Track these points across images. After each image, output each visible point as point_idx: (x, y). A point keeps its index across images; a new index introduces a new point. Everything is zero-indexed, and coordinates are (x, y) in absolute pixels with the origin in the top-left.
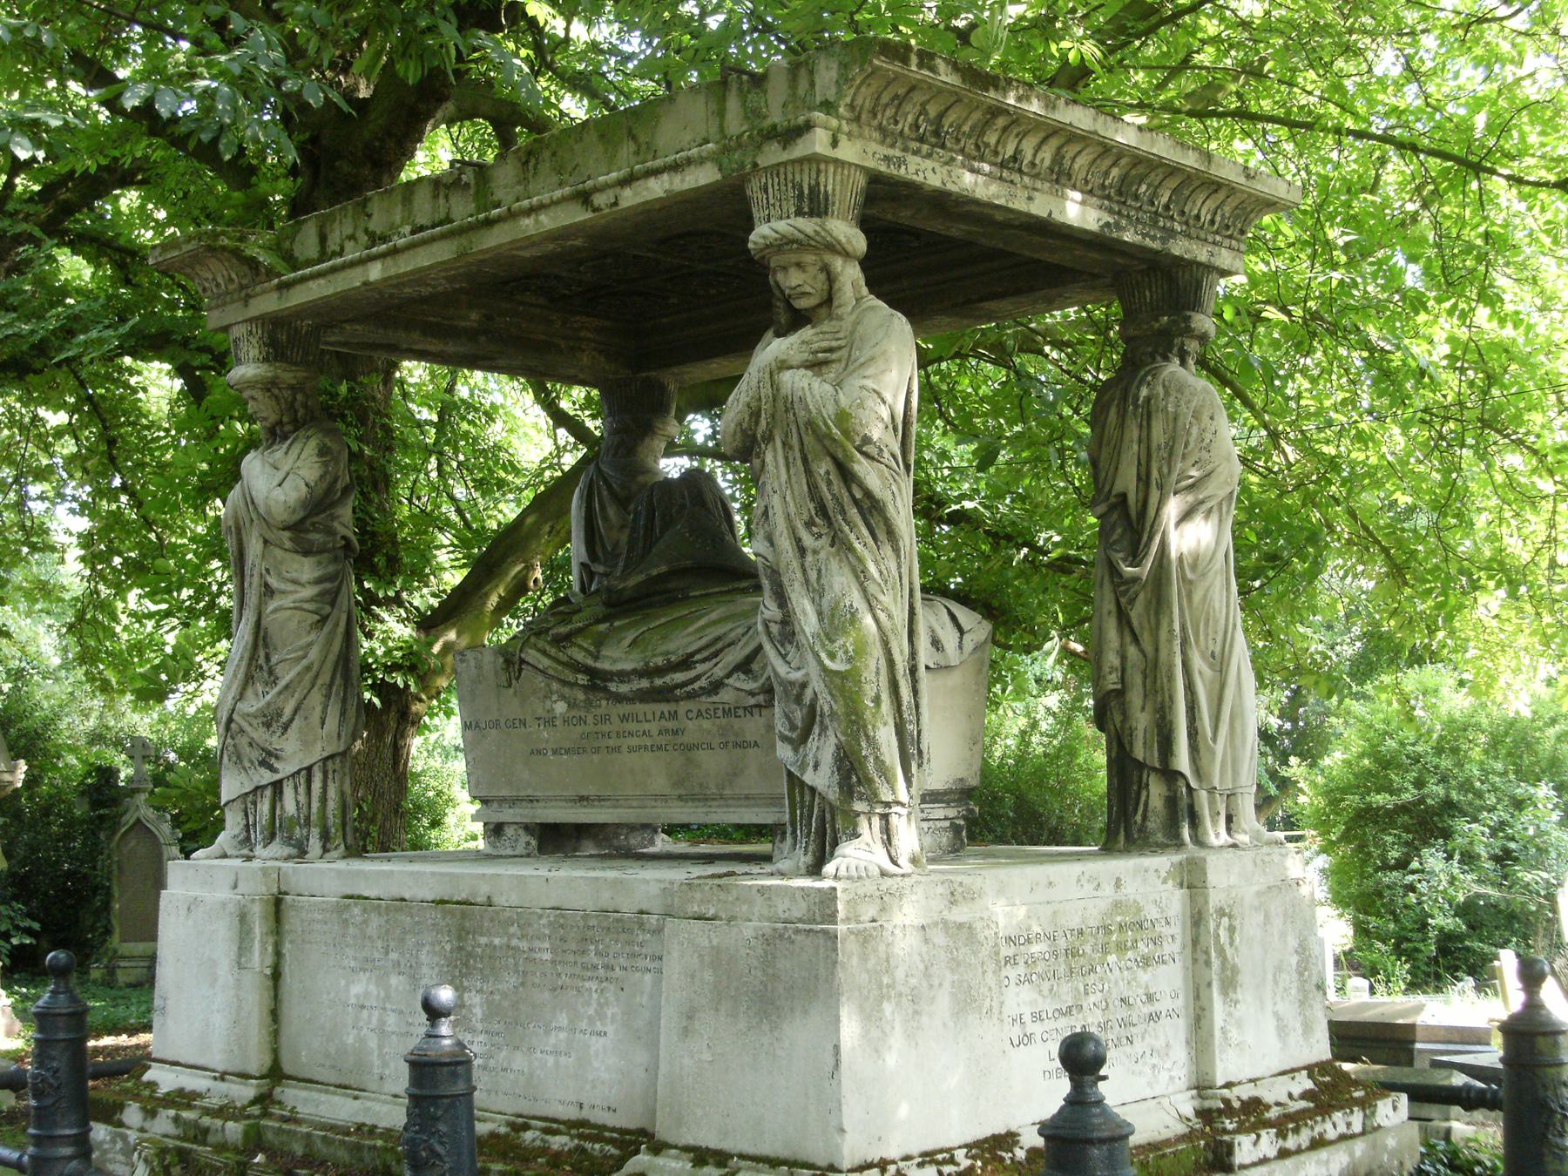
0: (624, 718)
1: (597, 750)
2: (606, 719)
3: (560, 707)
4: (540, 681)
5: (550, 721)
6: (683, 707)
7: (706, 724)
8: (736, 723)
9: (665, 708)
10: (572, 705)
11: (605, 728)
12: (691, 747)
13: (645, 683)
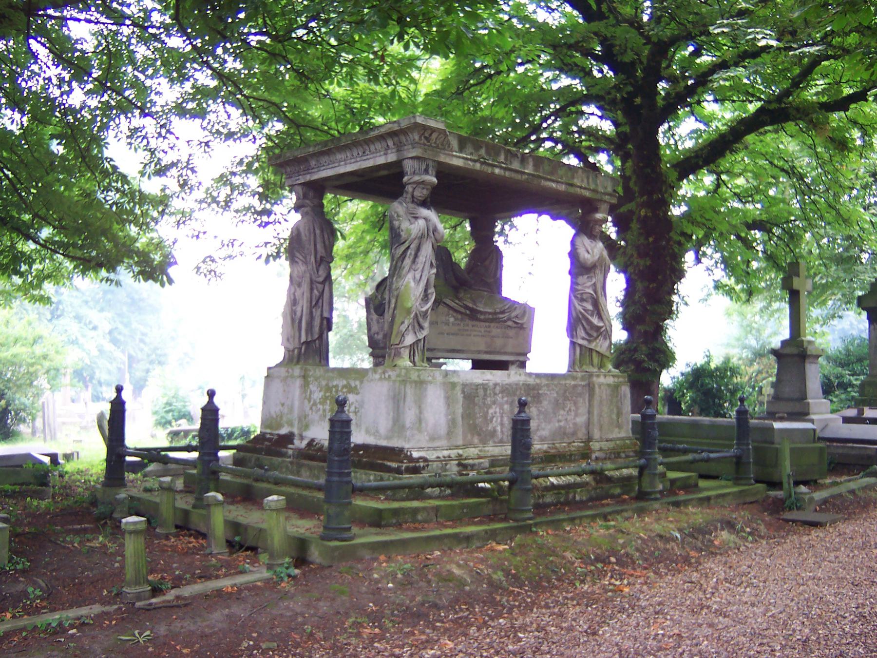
0: (473, 326)
1: (462, 335)
2: (468, 325)
3: (452, 320)
4: (446, 309)
5: (447, 324)
6: (492, 325)
7: (499, 330)
8: (507, 331)
9: (487, 324)
10: (456, 319)
11: (466, 328)
12: (493, 337)
13: (491, 316)
